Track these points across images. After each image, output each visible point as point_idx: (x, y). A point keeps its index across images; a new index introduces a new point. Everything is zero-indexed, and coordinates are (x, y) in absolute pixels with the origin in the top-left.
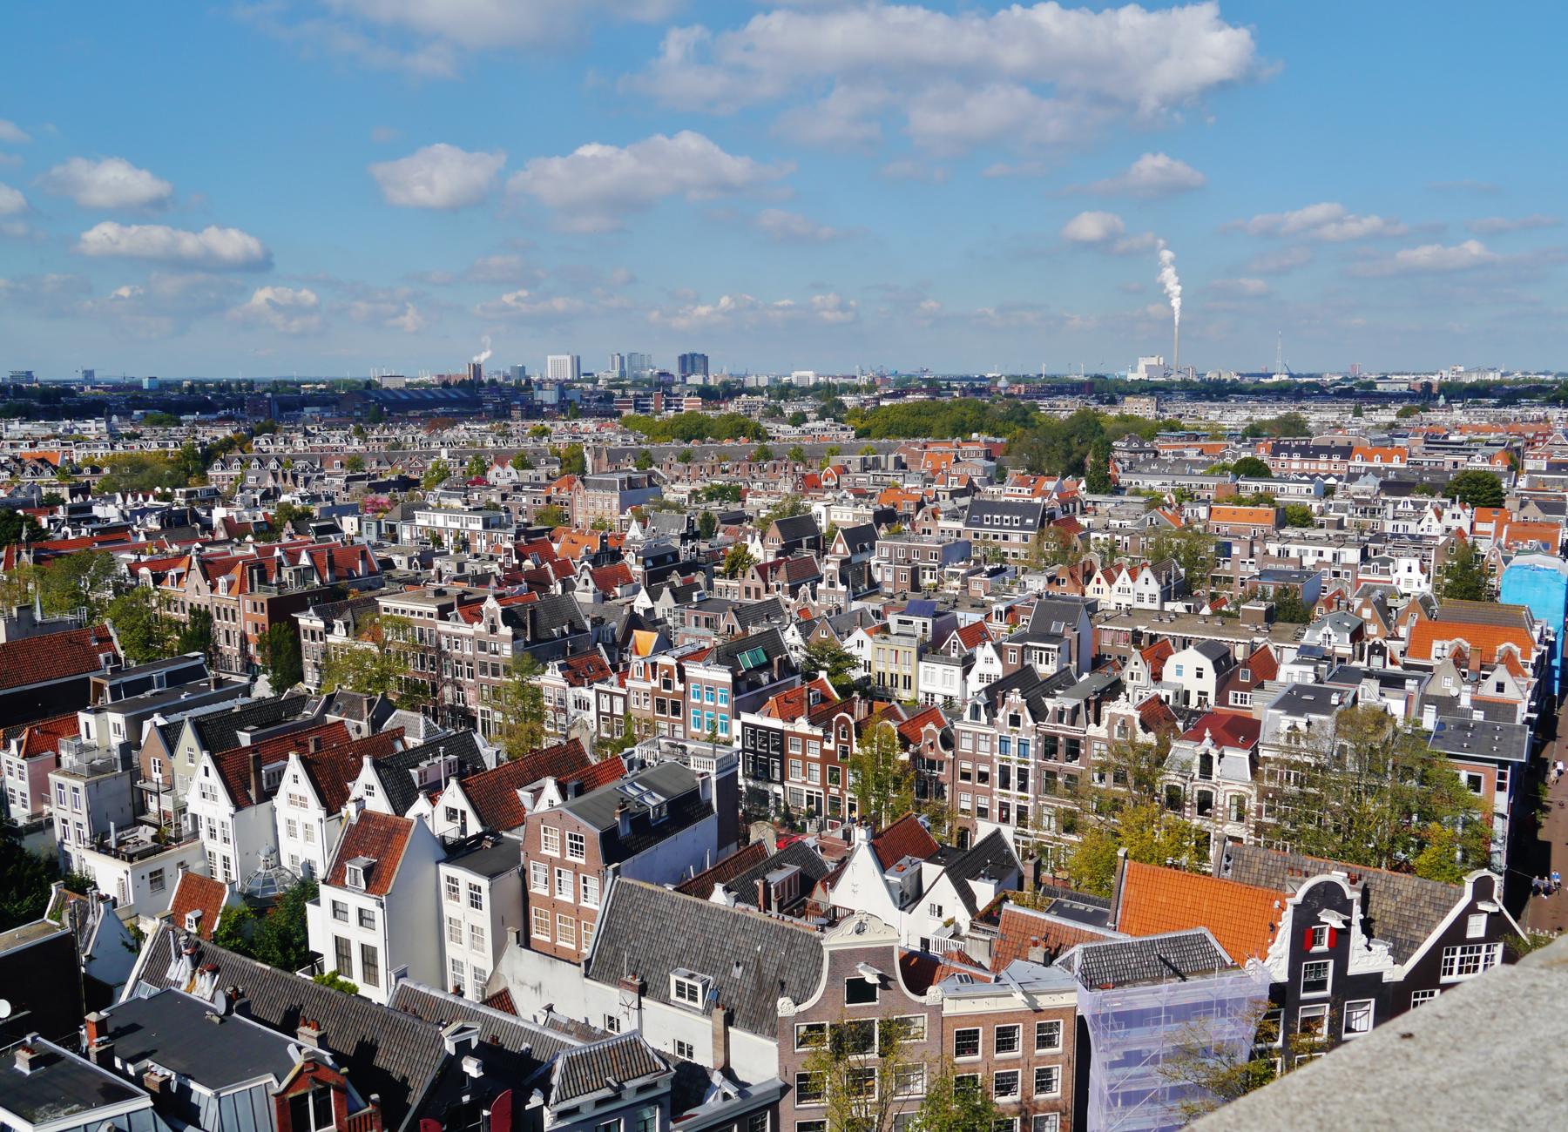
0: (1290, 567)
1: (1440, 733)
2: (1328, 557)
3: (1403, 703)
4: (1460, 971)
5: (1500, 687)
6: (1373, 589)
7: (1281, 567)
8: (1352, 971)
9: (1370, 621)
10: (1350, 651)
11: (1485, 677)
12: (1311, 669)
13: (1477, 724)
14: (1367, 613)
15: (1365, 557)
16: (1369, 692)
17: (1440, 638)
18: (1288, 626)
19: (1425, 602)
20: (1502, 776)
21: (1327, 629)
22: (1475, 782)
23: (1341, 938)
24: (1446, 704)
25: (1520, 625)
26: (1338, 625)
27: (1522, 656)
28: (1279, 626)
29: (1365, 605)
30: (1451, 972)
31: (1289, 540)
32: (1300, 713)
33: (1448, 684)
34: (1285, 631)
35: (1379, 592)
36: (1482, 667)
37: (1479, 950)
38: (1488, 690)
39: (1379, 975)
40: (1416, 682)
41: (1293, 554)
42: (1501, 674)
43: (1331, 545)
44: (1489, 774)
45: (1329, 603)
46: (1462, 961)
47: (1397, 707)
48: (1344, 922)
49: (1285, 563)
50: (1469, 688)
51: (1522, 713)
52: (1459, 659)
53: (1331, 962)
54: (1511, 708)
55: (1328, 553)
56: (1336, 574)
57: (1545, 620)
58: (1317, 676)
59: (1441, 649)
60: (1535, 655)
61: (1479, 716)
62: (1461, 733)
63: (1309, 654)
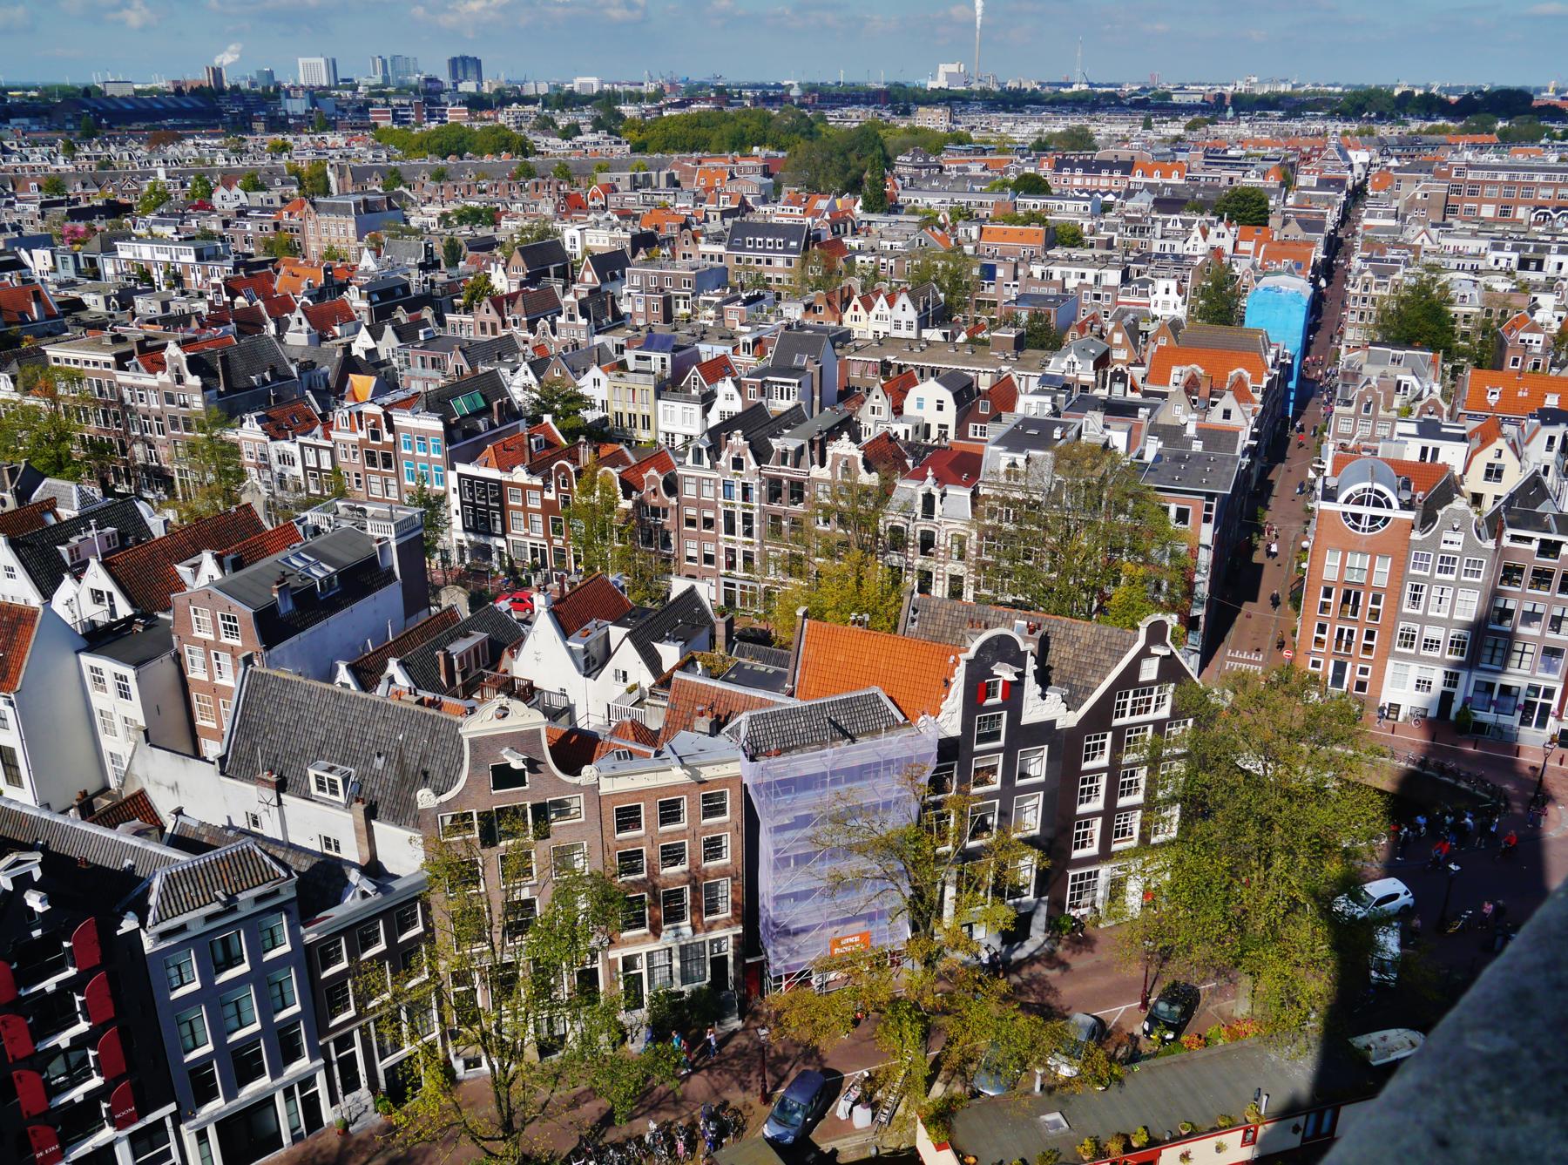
0: (1053, 291)
1: (1156, 466)
2: (1090, 279)
3: (1125, 435)
4: (1132, 713)
5: (1227, 414)
6: (1126, 313)
7: (1044, 290)
8: (1025, 720)
9: (1119, 346)
10: (1093, 379)
11: (1214, 404)
12: (1048, 399)
13: (1198, 455)
14: (1118, 338)
15: (1126, 279)
16: (1093, 426)
17: (1179, 364)
18: (1039, 353)
19: (1175, 325)
20: (1209, 508)
21: (1072, 357)
22: (1182, 516)
23: (1014, 691)
24: (1171, 434)
25: (1257, 350)
26: (1082, 352)
27: (1253, 380)
28: (1029, 353)
29: (1117, 329)
30: (1123, 715)
31: (1054, 260)
32: (1020, 451)
33: (1179, 413)
34: (1034, 358)
35: (1131, 316)
36: (1212, 394)
37: (1151, 692)
38: (1215, 418)
39: (1053, 722)
40: (1148, 411)
41: (1057, 277)
42: (1228, 401)
43: (1093, 267)
44: (1196, 506)
45: (1082, 328)
46: (1134, 703)
47: (1119, 439)
48: (1017, 674)
49: (1048, 286)
50: (1195, 416)
51: (1244, 440)
52: (1191, 386)
53: (1005, 714)
54: (1233, 435)
55: (1091, 274)
56: (1097, 297)
57: (1282, 344)
58: (1054, 407)
59: (1177, 374)
60: (1266, 379)
61: (1197, 446)
62: (1176, 465)
63: (1051, 384)
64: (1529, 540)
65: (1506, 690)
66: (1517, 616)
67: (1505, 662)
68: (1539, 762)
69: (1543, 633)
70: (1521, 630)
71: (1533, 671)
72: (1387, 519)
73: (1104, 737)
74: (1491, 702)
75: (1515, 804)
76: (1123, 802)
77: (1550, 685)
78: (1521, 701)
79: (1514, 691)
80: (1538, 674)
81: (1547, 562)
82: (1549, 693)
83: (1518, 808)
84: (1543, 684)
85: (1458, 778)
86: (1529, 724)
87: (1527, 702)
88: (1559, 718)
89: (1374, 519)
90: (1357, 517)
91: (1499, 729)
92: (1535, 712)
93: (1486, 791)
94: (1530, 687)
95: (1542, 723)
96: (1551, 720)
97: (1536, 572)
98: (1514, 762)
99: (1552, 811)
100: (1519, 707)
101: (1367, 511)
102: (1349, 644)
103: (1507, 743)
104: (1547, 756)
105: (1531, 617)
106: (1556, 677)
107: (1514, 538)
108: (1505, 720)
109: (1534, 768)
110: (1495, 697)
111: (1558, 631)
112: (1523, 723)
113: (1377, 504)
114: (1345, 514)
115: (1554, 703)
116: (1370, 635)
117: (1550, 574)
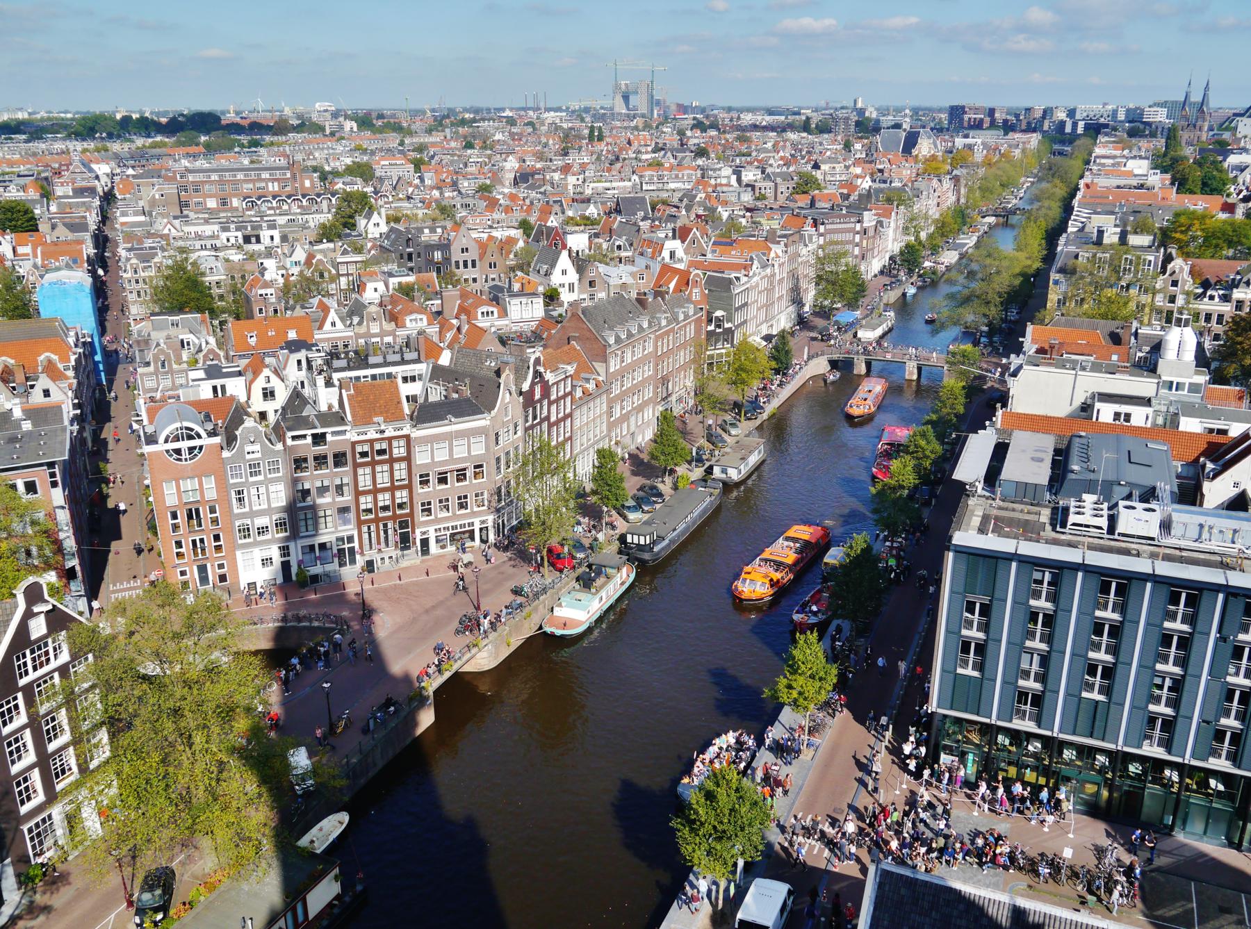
4: (35, 669)
5: (47, 393)
11: (32, 387)
13: (29, 433)
20: (53, 475)
22: (31, 487)
25: (57, 335)
27: (61, 360)
30: (27, 673)
36: (27, 379)
37: (46, 645)
38: (37, 398)
42: (43, 382)
44: (41, 477)
46: (34, 660)
50: (17, 401)
51: (69, 411)
54: (57, 409)
57: (78, 326)
60: (73, 358)
61: (27, 426)
62: (11, 446)
64: (304, 436)
65: (323, 546)
66: (314, 492)
67: (316, 527)
68: (358, 589)
69: (333, 499)
70: (320, 501)
71: (336, 528)
72: (201, 448)
73: (15, 699)
74: (316, 558)
75: (352, 624)
76: (52, 747)
77: (349, 533)
78: (335, 551)
79: (328, 545)
80: (340, 528)
81: (320, 449)
82: (350, 539)
83: (355, 625)
84: (345, 534)
85: (311, 620)
86: (345, 564)
87: (339, 550)
88: (362, 554)
89: (191, 449)
90: (178, 452)
91: (327, 575)
92: (345, 556)
93: (333, 623)
94: (338, 539)
95: (353, 561)
96: (358, 557)
97: (316, 458)
98: (343, 595)
99: (376, 618)
100: (335, 556)
101: (184, 445)
102: (203, 550)
103: (336, 583)
104: (362, 583)
105: (323, 490)
106: (351, 527)
107: (294, 438)
108: (329, 567)
109: (357, 594)
110: (317, 554)
111: (342, 495)
112: (341, 565)
113: (190, 437)
114: (167, 451)
115: (356, 544)
116: (217, 538)
117: (325, 457)
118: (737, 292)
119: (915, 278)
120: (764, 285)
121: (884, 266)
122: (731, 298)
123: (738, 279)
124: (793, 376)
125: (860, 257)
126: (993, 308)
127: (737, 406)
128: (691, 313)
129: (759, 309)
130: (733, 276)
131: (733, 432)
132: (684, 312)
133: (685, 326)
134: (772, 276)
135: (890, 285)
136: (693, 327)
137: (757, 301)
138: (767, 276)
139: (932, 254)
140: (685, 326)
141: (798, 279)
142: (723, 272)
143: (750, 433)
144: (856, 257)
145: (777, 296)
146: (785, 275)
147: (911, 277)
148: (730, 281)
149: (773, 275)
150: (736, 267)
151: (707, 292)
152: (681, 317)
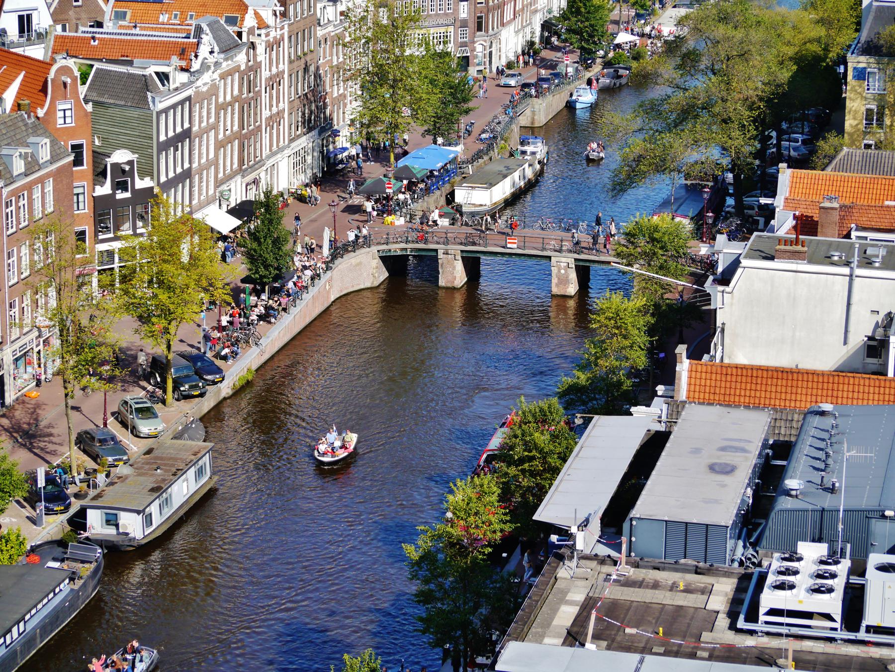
118: (161, 106)
119: (597, 68)
120: (231, 90)
121: (531, 44)
122: (147, 121)
123: (164, 77)
124: (294, 297)
125: (472, 25)
126: (736, 133)
127: (159, 366)
128: (44, 154)
129: (219, 145)
130: (152, 70)
131: (145, 427)
132: (24, 157)
133: (29, 187)
134: (250, 69)
135: (536, 85)
136: (49, 187)
137: (215, 127)
138: (237, 69)
139: (639, 16)
140: (29, 187)
141: (317, 76)
142: (130, 63)
143: (186, 428)
144: (464, 24)
145: (266, 113)
146: (284, 66)
147: (588, 67)
148: (145, 84)
149: (255, 68)
150: (160, 51)
151: (89, 107)
152: (19, 166)
